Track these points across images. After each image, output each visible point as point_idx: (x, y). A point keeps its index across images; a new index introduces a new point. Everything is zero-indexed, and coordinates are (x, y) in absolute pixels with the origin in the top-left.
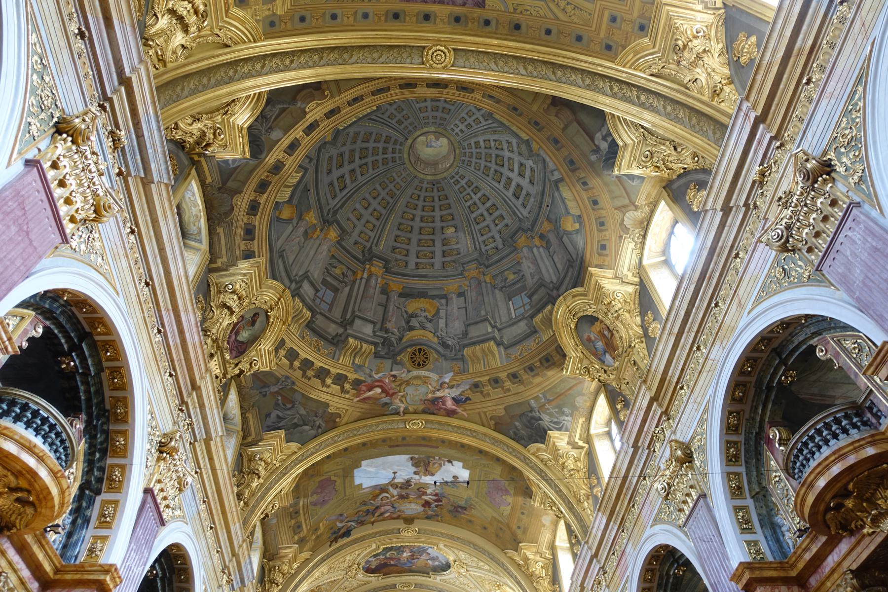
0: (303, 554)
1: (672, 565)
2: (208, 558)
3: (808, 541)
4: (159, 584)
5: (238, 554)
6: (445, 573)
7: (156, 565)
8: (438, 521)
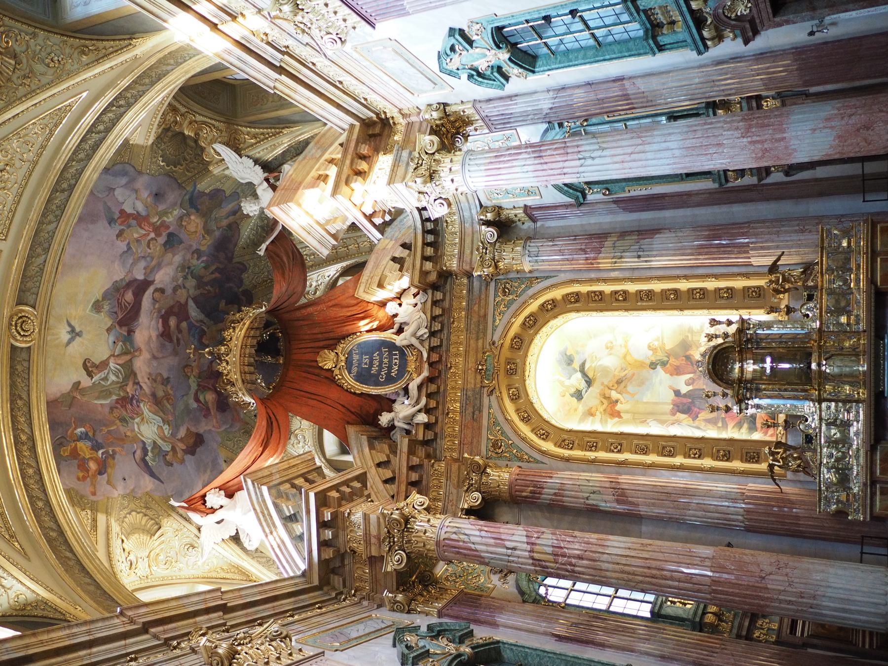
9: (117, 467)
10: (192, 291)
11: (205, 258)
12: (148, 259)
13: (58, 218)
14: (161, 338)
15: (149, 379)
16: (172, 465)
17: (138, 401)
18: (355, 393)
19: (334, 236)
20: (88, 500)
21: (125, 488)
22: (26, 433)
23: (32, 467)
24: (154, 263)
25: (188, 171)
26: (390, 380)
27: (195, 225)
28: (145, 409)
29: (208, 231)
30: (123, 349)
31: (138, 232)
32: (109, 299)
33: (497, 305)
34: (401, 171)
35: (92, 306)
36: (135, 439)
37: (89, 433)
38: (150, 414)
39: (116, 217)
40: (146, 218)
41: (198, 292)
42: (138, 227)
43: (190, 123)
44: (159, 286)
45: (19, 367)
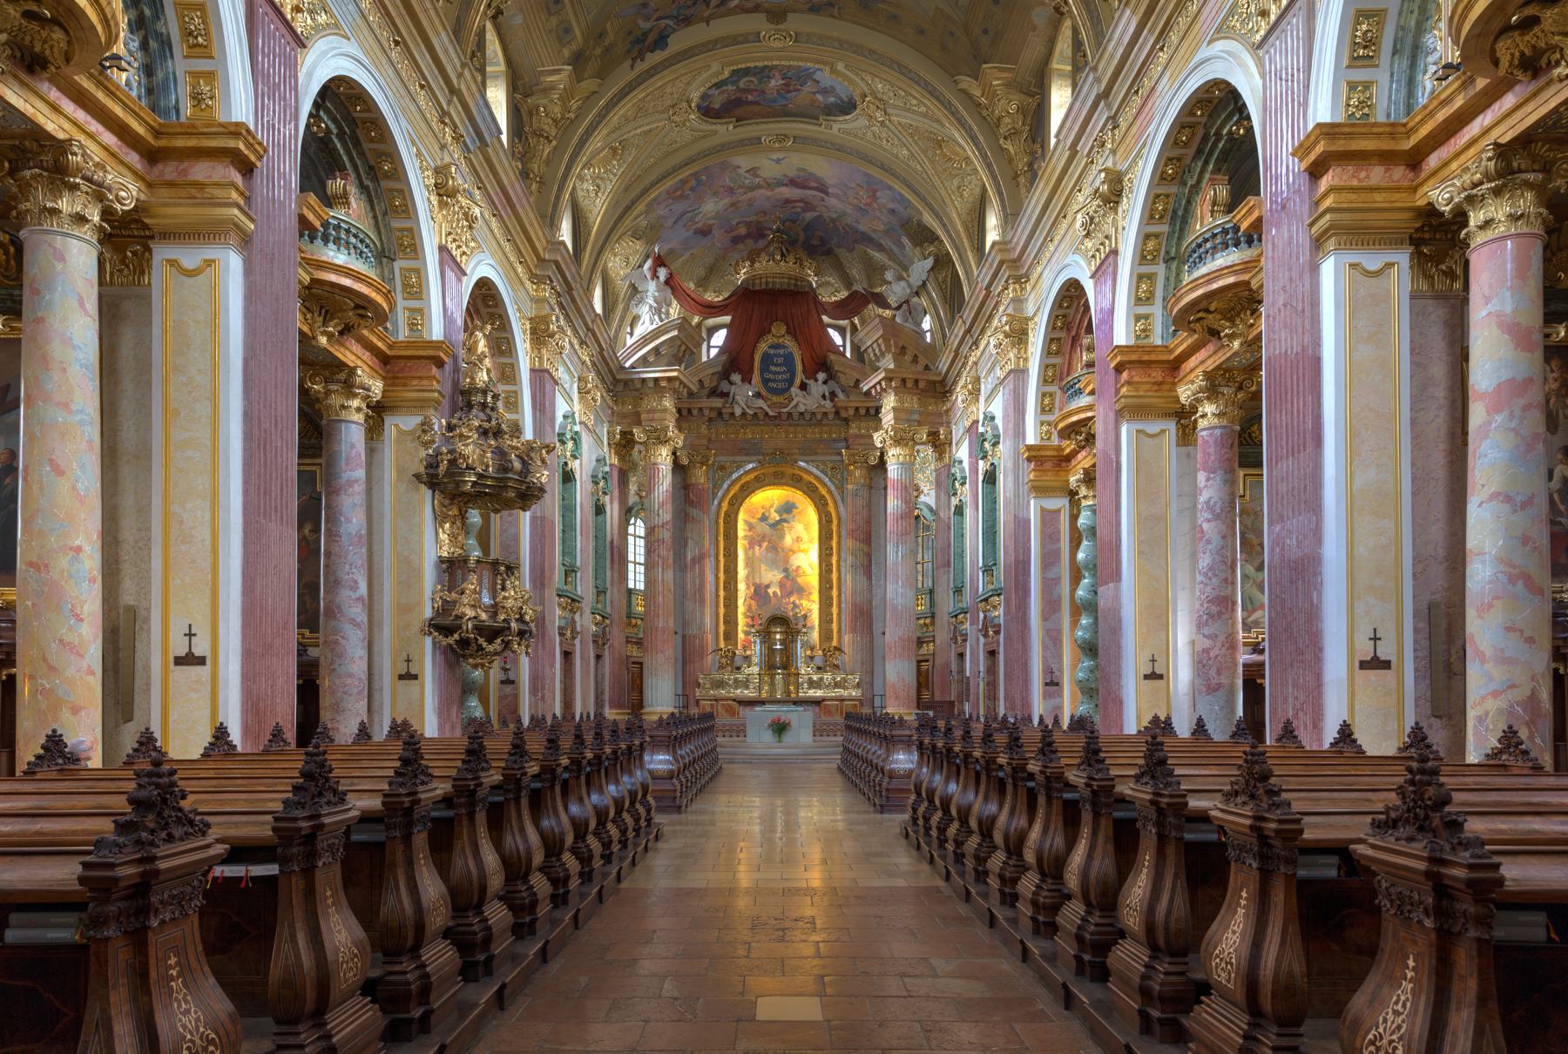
0: (584, 83)
1: (1230, 116)
2: (407, 99)
3: (1456, 85)
4: (339, 146)
5: (460, 90)
6: (848, 117)
7: (321, 113)
8: (833, 16)
18: (753, 353)
19: (866, 350)
26: (765, 381)
28: (727, 201)
29: (875, 231)
33: (824, 463)
34: (903, 416)
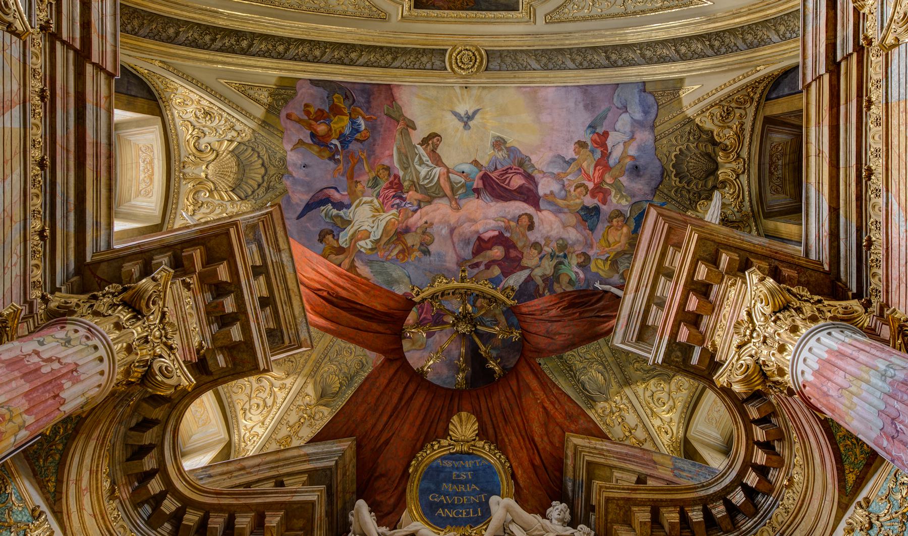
9: (320, 161)
10: (538, 272)
11: (582, 276)
12: (563, 193)
13: (580, 67)
14: (475, 237)
15: (426, 223)
16: (321, 240)
17: (398, 205)
20: (282, 106)
21: (295, 165)
22: (358, 59)
23: (322, 57)
24: (561, 203)
25: (676, 191)
27: (617, 239)
30: (457, 184)
31: (589, 165)
32: (509, 157)
35: (498, 137)
36: (353, 195)
37: (359, 135)
38: (384, 223)
39: (598, 131)
40: (607, 168)
41: (539, 281)
42: (595, 162)
43: (734, 170)
44: (536, 220)
45: (424, 59)
